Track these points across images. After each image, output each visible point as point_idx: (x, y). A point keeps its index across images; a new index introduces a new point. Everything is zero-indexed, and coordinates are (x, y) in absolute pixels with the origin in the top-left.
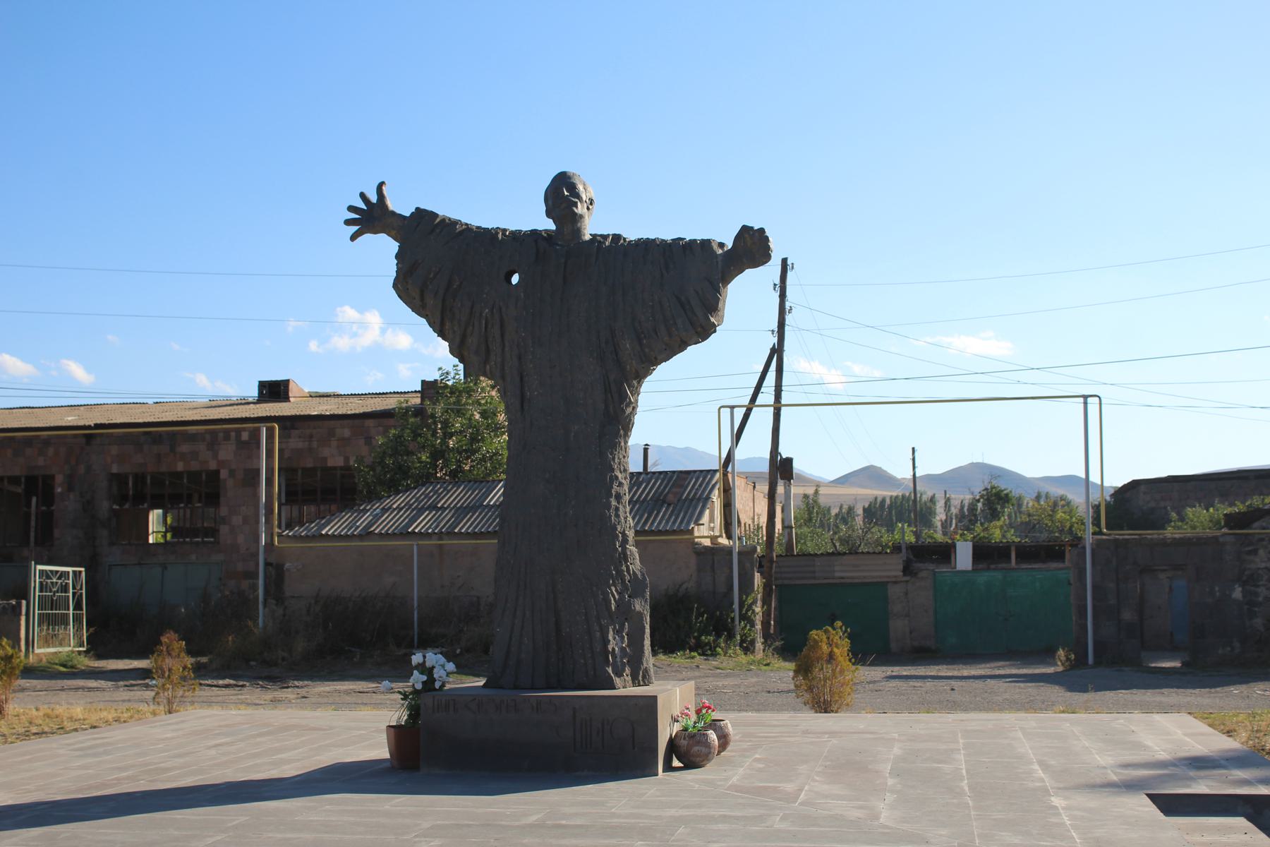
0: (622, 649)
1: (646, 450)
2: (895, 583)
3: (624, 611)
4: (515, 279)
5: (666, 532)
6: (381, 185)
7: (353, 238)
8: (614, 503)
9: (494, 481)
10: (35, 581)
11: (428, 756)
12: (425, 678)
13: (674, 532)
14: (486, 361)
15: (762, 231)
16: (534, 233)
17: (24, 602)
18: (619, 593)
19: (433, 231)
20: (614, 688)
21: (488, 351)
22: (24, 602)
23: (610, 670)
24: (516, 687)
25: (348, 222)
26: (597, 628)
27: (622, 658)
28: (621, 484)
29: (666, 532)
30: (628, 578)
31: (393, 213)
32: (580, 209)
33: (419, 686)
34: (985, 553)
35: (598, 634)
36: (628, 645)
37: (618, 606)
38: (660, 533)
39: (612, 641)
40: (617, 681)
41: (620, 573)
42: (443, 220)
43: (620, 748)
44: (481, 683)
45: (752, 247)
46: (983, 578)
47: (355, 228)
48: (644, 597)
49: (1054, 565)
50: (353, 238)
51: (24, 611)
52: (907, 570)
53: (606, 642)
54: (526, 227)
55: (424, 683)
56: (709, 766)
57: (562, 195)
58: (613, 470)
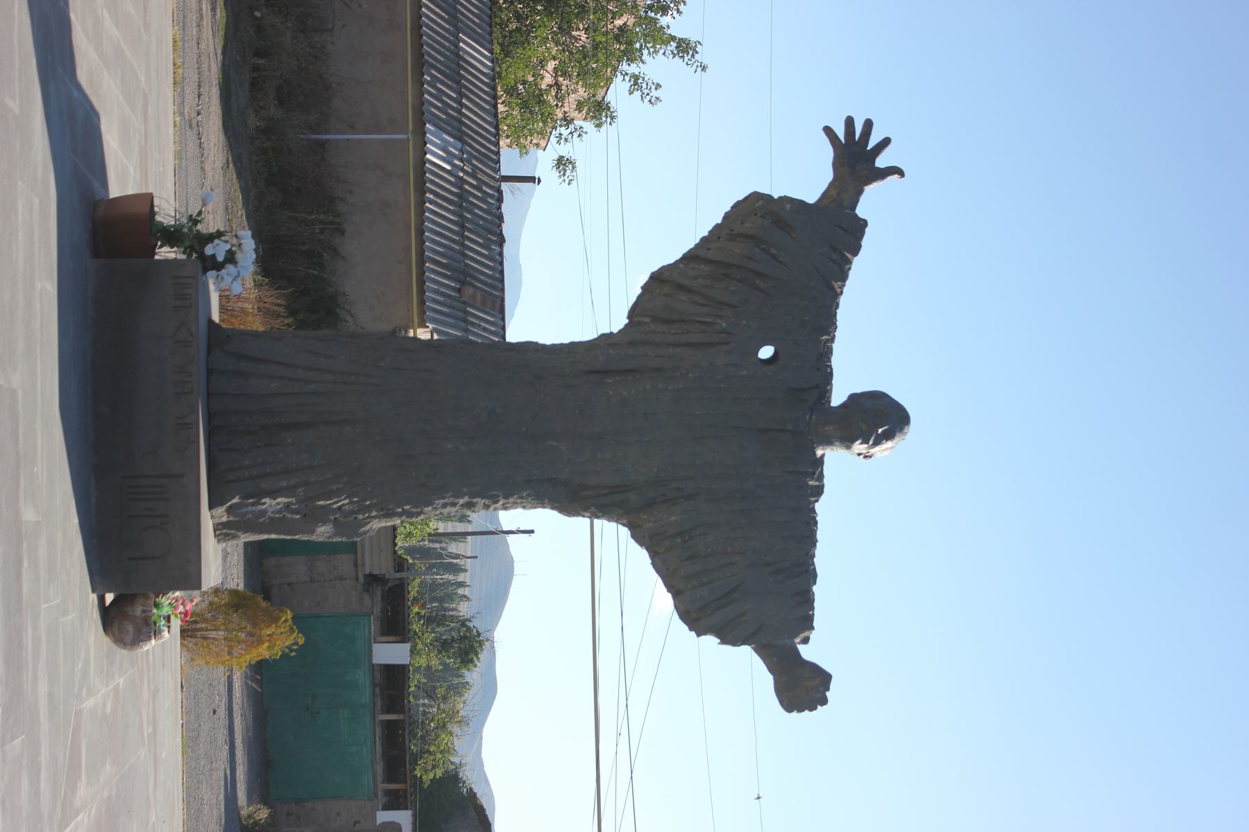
0: (264, 512)
1: (531, 179)
2: (356, 564)
4: (766, 352)
5: (421, 292)
6: (899, 172)
7: (828, 131)
8: (461, 501)
9: (491, 42)
11: (110, 247)
12: (220, 258)
13: (422, 302)
14: (655, 319)
15: (824, 701)
16: (825, 378)
18: (340, 508)
19: (834, 249)
20: (211, 508)
21: (669, 322)
23: (236, 500)
24: (210, 372)
25: (850, 122)
27: (252, 512)
29: (421, 292)
30: (360, 517)
31: (860, 192)
32: (858, 447)
33: (209, 250)
34: (394, 676)
35: (284, 484)
36: (272, 519)
37: (323, 507)
38: (421, 282)
39: (274, 502)
40: (221, 511)
42: (850, 262)
43: (130, 563)
44: (216, 317)
45: (802, 687)
46: (362, 678)
47: (841, 133)
48: (335, 535)
49: (379, 768)
50: (828, 131)
52: (373, 580)
53: (273, 494)
54: (836, 361)
55: (214, 256)
56: (106, 640)
57: (878, 418)
58: (506, 497)
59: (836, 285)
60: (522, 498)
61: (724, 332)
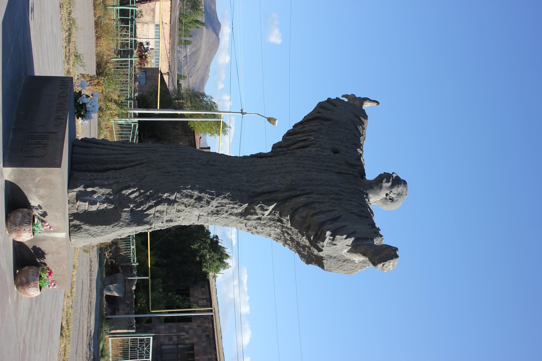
3: (120, 202)
10: (144, 336)
15: (397, 256)
17: (134, 331)
22: (134, 331)
23: (81, 188)
26: (110, 182)
28: (208, 203)
35: (106, 183)
41: (148, 199)
45: (383, 255)
51: (130, 331)
53: (102, 186)
58: (217, 196)
59: (360, 128)
60: (225, 198)
61: (313, 140)
